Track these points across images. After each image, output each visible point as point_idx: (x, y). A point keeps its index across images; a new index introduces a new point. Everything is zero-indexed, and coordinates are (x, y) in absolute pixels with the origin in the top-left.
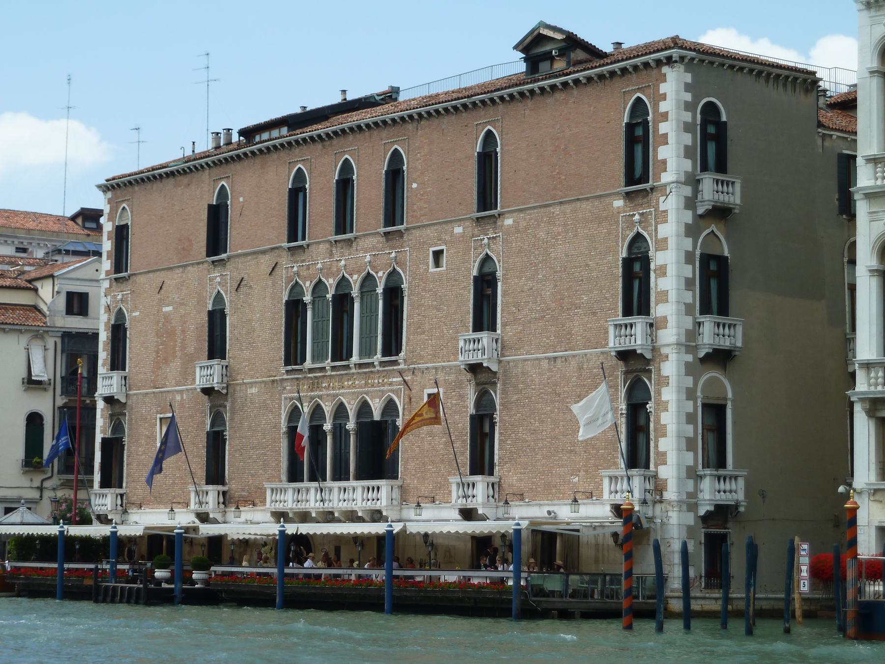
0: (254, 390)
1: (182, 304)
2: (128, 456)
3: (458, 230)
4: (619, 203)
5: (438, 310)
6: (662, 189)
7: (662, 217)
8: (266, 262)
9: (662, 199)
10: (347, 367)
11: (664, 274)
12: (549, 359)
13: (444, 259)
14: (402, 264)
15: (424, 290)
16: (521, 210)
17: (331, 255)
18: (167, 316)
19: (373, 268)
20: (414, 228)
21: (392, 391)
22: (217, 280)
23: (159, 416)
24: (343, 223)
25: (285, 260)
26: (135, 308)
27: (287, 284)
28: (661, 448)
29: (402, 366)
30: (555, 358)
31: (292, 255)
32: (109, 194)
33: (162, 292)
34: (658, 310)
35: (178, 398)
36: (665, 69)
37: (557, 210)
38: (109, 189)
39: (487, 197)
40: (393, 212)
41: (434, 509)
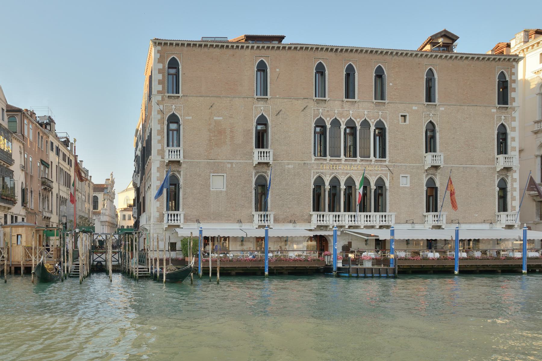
0: (290, 166)
1: (231, 117)
2: (184, 195)
3: (415, 108)
4: (494, 110)
5: (405, 141)
6: (513, 109)
7: (514, 119)
8: (300, 104)
9: (513, 112)
10: (356, 160)
11: (514, 141)
12: (464, 168)
13: (401, 119)
14: (385, 118)
15: (397, 131)
16: (448, 105)
17: (342, 107)
18: (217, 123)
19: (368, 117)
20: (391, 103)
21: (382, 174)
22: (261, 108)
23: (211, 174)
24: (349, 93)
25: (312, 105)
26: (188, 115)
27: (314, 117)
28: (513, 205)
29: (387, 163)
30: (466, 167)
31: (318, 103)
32: (159, 48)
33: (212, 109)
34: (510, 153)
35: (229, 166)
36: (514, 63)
37: (466, 108)
38: (160, 44)
39: (430, 97)
40: (380, 94)
41: (406, 225)
